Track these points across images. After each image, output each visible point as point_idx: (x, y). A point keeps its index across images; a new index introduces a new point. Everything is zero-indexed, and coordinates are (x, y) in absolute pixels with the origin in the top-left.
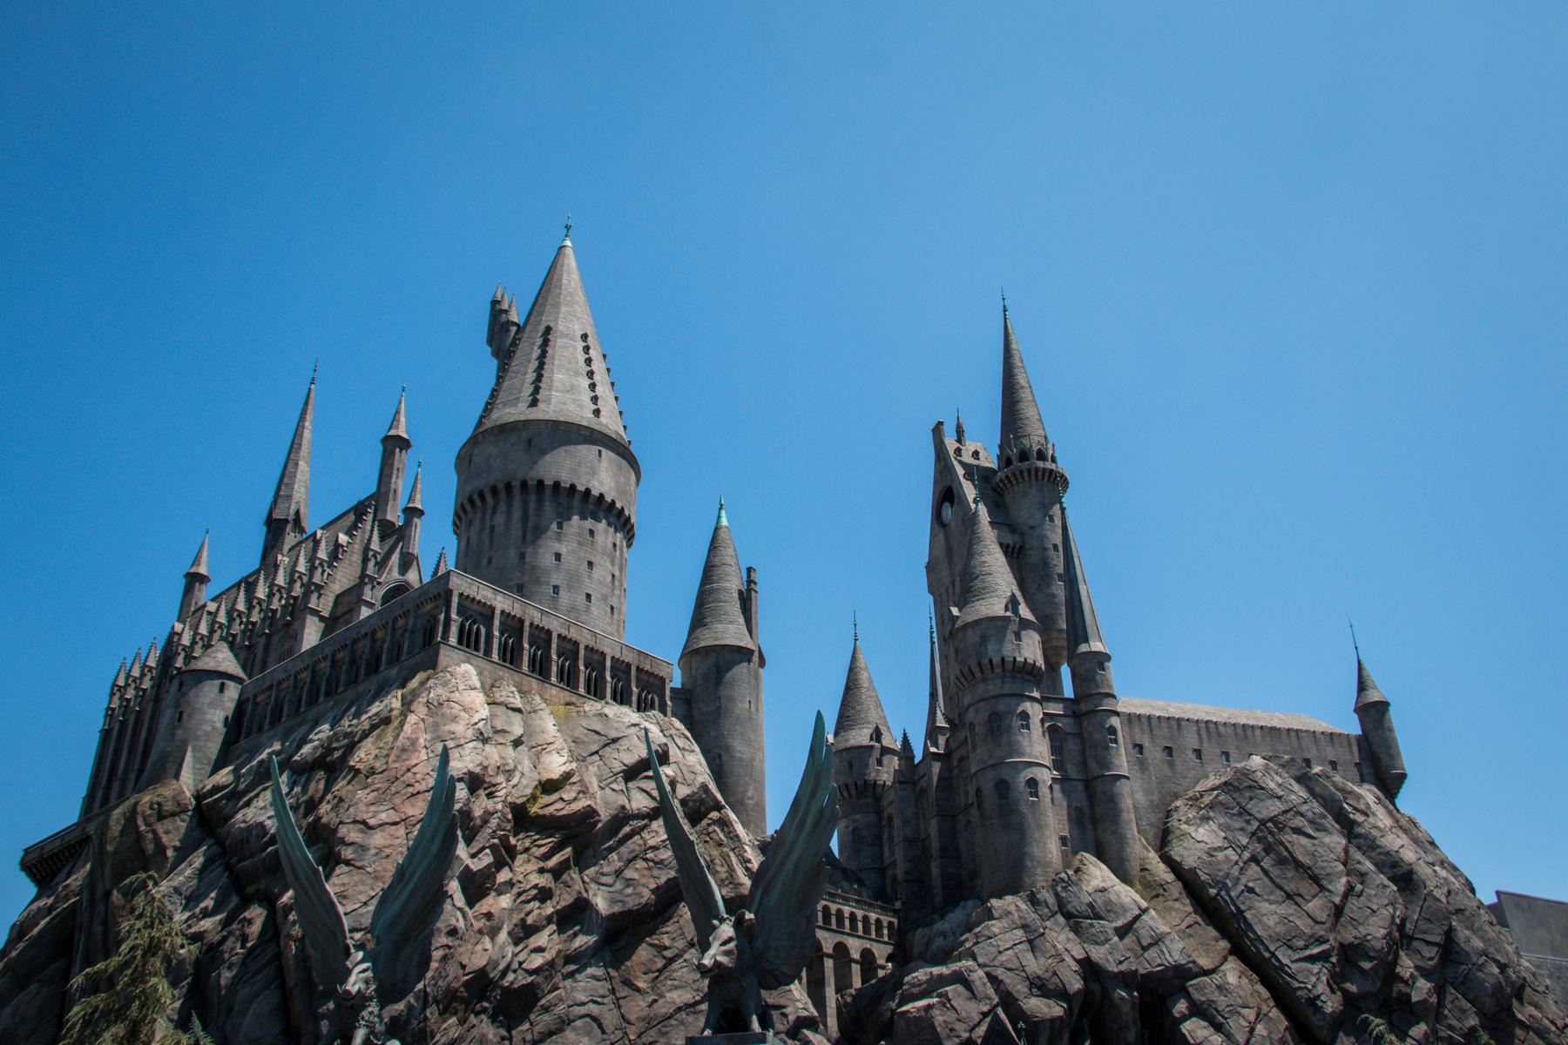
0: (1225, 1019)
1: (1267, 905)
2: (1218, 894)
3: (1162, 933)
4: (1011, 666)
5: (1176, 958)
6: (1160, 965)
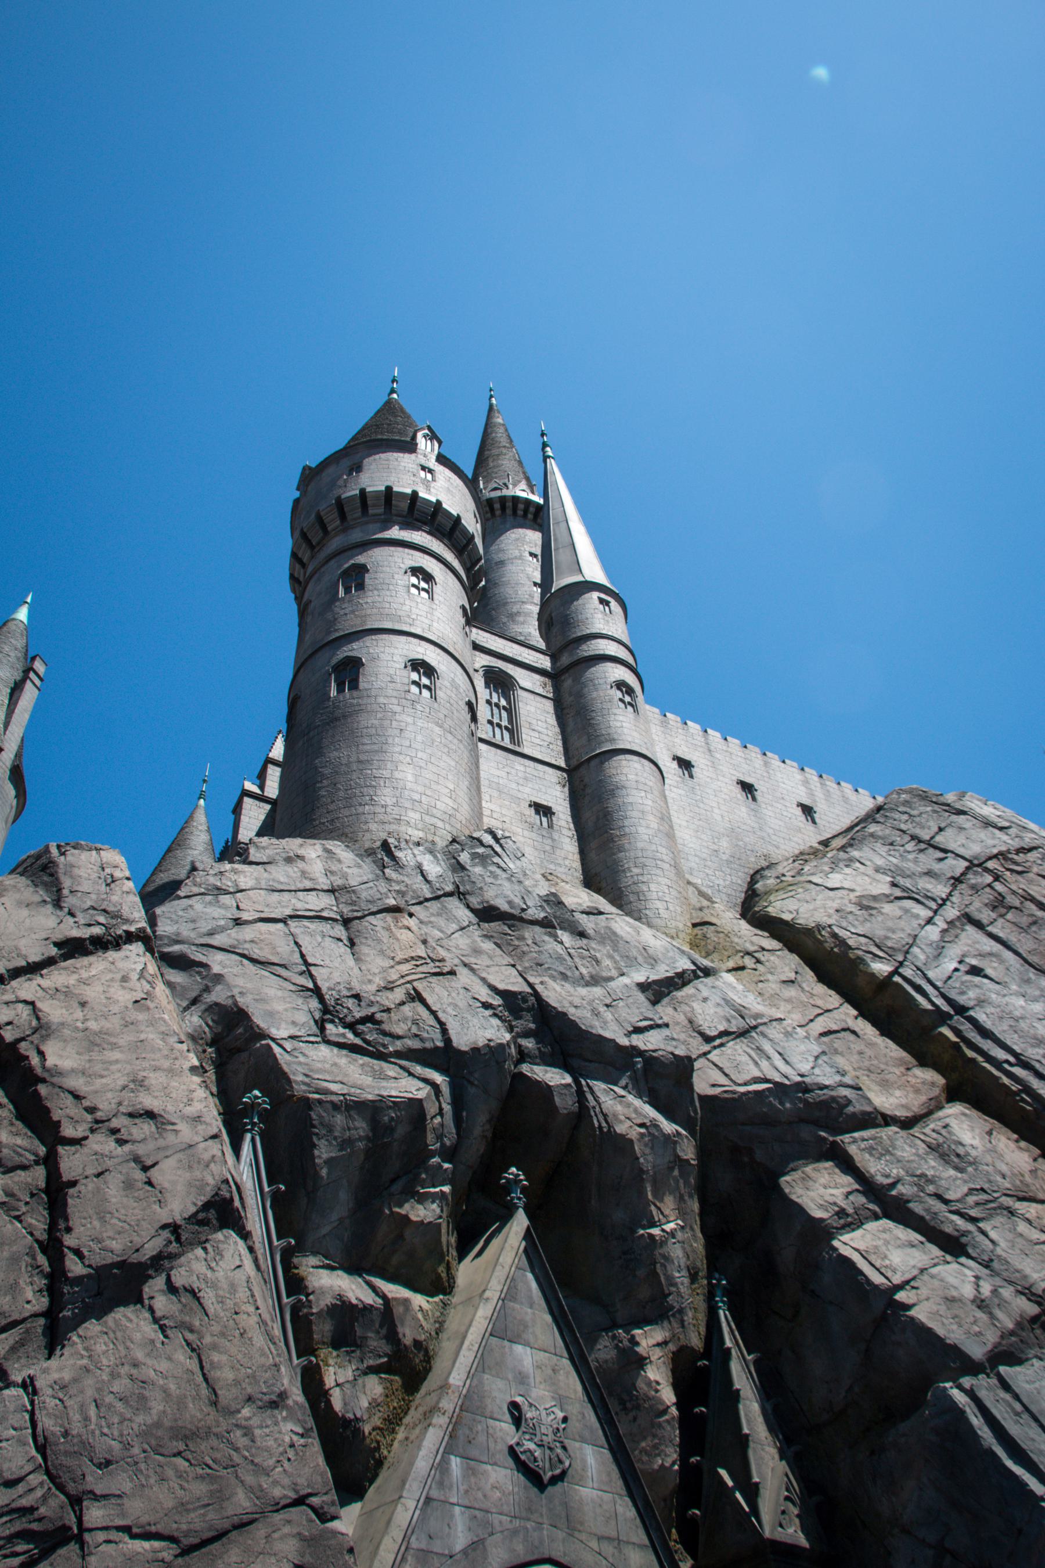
0: (973, 1220)
1: (1021, 1002)
2: (896, 972)
3: (757, 1016)
4: (405, 505)
5: (805, 1067)
6: (756, 1080)
